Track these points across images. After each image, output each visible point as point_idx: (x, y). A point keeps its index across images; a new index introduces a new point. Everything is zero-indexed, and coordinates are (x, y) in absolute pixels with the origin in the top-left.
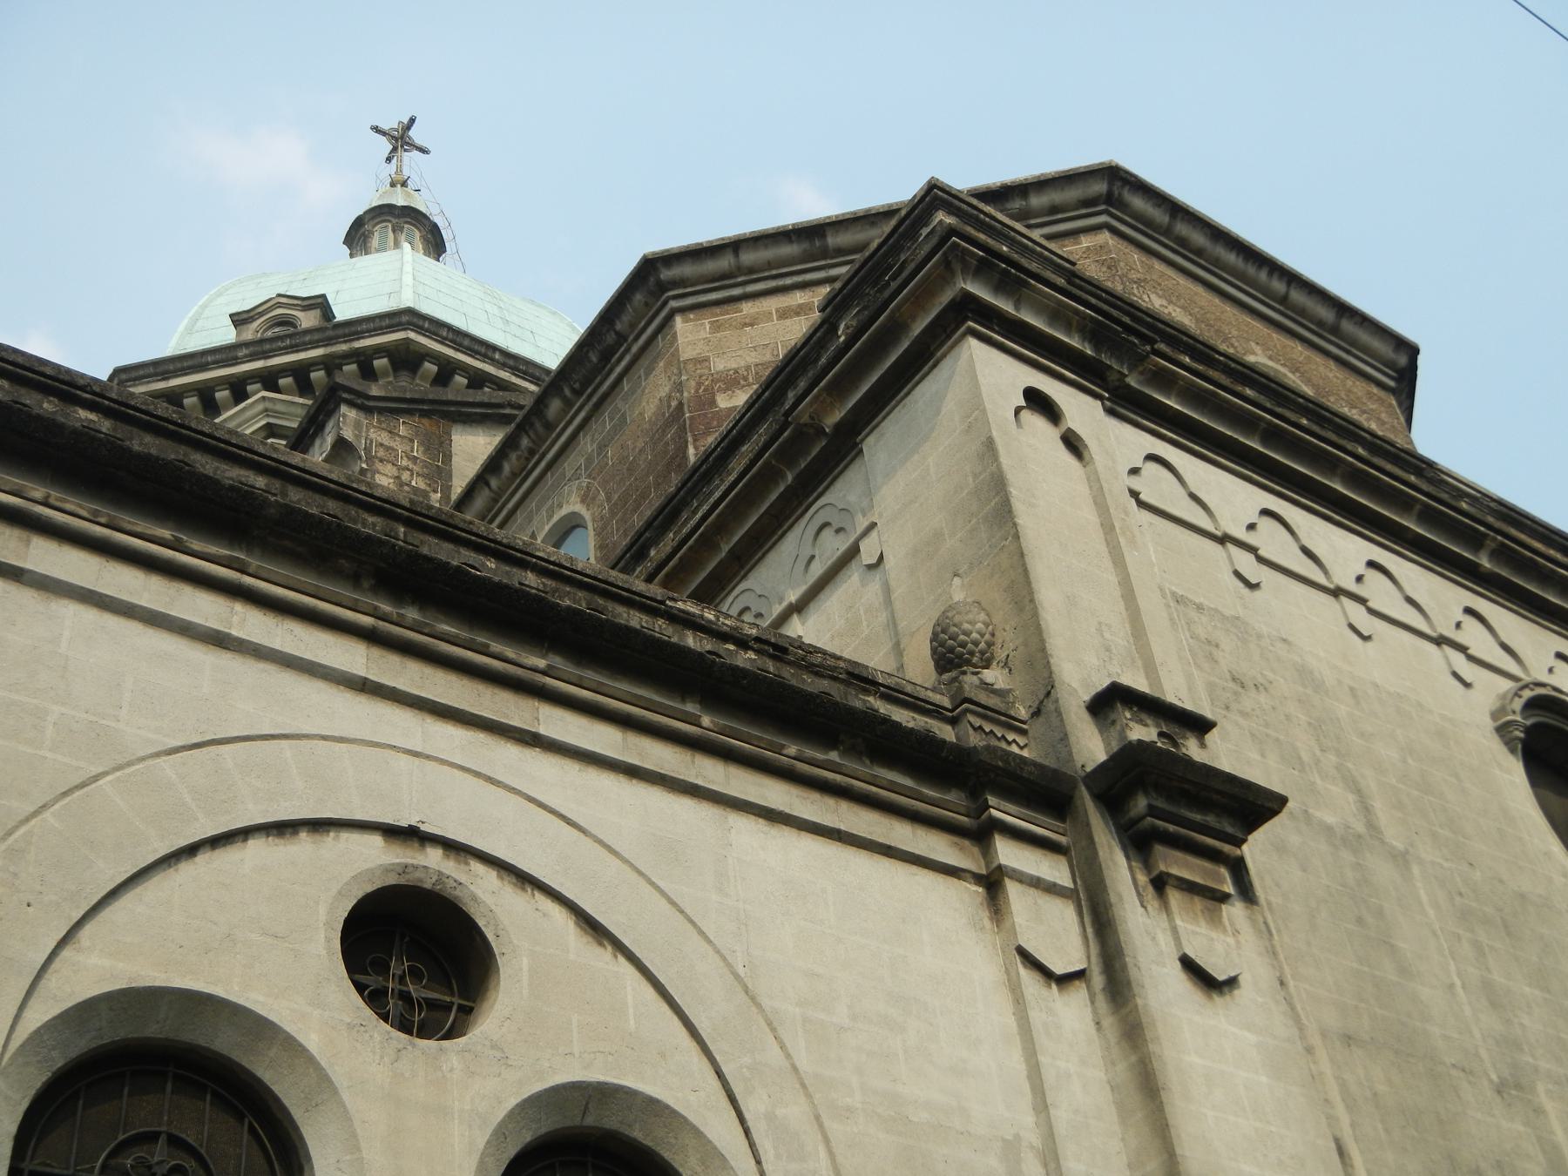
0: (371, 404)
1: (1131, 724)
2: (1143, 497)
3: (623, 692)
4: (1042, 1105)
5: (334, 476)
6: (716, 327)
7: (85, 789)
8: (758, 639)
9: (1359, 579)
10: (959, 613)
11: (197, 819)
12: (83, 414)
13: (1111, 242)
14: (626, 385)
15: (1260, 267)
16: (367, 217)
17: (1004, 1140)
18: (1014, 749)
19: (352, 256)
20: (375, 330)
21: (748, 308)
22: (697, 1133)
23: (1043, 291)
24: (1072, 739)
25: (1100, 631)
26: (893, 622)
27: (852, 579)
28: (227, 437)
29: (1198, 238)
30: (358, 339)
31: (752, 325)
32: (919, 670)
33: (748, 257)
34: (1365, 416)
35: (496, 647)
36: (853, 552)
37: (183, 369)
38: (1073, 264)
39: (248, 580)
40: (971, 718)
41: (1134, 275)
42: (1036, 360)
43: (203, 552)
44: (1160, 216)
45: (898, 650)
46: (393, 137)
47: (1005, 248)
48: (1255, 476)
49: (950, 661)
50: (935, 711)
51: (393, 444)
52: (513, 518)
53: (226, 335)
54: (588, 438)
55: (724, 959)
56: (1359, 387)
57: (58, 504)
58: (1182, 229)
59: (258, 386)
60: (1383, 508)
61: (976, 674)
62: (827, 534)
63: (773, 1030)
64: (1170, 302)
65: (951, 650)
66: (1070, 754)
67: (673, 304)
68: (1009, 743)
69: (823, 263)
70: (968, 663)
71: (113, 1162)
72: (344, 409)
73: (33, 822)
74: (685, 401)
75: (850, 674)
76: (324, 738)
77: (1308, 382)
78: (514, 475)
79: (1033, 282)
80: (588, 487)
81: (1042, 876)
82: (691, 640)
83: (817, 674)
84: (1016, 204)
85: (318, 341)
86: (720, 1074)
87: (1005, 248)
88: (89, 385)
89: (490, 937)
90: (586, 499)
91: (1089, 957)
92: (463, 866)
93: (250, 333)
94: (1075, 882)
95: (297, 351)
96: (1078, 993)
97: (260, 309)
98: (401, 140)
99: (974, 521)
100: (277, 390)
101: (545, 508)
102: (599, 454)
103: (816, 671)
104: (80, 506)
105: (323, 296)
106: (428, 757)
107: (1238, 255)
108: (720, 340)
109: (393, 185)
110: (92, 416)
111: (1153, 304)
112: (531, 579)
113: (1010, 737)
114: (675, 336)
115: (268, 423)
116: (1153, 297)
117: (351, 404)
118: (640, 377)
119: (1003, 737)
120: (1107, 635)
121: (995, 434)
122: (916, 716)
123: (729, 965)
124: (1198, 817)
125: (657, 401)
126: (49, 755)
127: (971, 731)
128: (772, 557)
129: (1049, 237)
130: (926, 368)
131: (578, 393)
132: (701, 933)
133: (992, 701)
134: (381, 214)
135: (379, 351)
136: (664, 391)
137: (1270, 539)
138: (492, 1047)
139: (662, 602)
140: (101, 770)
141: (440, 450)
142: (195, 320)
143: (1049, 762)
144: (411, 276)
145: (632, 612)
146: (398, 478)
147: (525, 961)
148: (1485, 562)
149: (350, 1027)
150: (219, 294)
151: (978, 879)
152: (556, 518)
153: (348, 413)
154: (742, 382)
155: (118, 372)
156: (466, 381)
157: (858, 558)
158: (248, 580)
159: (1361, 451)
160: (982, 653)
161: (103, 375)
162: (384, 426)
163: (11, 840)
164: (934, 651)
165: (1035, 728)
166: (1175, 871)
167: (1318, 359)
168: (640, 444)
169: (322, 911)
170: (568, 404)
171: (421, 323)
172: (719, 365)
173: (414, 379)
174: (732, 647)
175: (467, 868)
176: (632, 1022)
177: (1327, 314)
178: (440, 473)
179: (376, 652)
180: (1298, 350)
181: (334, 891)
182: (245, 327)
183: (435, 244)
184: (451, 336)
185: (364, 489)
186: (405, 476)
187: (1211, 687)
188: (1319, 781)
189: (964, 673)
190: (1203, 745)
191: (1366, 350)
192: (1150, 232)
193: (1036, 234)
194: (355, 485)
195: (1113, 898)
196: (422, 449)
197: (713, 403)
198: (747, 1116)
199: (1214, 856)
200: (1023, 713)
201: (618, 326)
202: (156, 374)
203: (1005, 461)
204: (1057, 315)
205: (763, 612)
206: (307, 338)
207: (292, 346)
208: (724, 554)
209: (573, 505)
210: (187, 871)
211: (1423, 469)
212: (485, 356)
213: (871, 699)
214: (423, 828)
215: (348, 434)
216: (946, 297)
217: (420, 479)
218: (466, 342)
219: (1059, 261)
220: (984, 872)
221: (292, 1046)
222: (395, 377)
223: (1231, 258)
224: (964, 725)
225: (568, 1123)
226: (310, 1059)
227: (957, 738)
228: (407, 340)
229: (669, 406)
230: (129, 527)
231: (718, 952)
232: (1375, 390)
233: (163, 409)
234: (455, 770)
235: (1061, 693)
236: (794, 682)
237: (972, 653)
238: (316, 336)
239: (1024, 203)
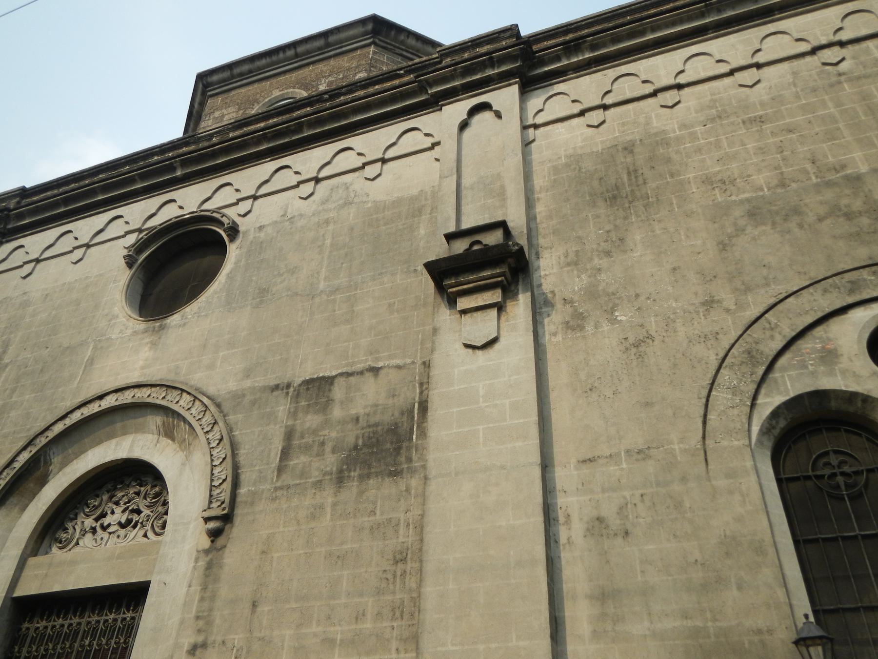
29: (245, 68)
44: (226, 74)
58: (237, 71)
107: (266, 58)
148: (179, 173)
191: (347, 39)
211: (187, 141)
223: (264, 62)
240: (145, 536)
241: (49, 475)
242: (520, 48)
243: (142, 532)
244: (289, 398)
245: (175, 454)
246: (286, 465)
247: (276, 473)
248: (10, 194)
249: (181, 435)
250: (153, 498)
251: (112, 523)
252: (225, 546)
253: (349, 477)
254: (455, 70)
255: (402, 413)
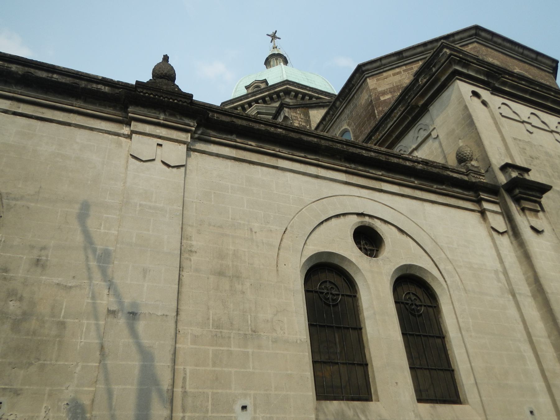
0: (291, 107)
1: (512, 172)
2: (503, 114)
3: (398, 178)
4: (501, 261)
5: (329, 136)
6: (378, 80)
7: (301, 212)
8: (422, 161)
9: (557, 127)
10: (463, 149)
11: (322, 216)
12: (279, 130)
13: (477, 45)
14: (356, 97)
15: (516, 46)
16: (269, 57)
17: (495, 270)
18: (482, 180)
19: (267, 68)
20: (279, 86)
21: (385, 74)
22: (430, 273)
23: (474, 66)
24: (497, 177)
25: (498, 149)
26: (443, 151)
27: (430, 142)
28: (307, 131)
29: (499, 41)
30: (275, 89)
31: (386, 79)
32: (452, 162)
33: (384, 62)
34: (545, 81)
35: (371, 171)
36: (430, 135)
37: (237, 101)
38: (478, 56)
39: (320, 163)
40: (472, 174)
41: (484, 54)
42: (473, 83)
43: (311, 158)
44: (489, 37)
45: (445, 157)
46: (272, 36)
47: (461, 55)
49: (462, 160)
50: (462, 173)
51: (297, 116)
52: (330, 131)
53: (244, 92)
54: (347, 110)
55: (429, 235)
56: (543, 74)
57: (281, 151)
58: (495, 39)
59: (254, 103)
61: (470, 163)
62: (421, 131)
63: (442, 250)
64: (494, 59)
65: (462, 158)
66: (497, 180)
67: (366, 76)
68: (481, 179)
69: (402, 61)
70: (467, 160)
71: (320, 287)
72: (285, 109)
73: (293, 220)
74: (372, 99)
75: (443, 167)
76: (341, 195)
77: (530, 74)
78: (329, 121)
79: (471, 64)
80: (349, 122)
81: (494, 210)
82: (408, 163)
83: (436, 168)
84: (451, 39)
85: (266, 90)
86: (433, 260)
87: (461, 55)
88: (279, 123)
89: (381, 235)
90: (349, 125)
91: (507, 227)
92: (373, 220)
93: (250, 90)
94: (502, 210)
95: (262, 94)
96: (506, 236)
97: (251, 84)
98: (274, 37)
99: (464, 126)
100: (259, 103)
101: (338, 128)
102: (351, 114)
103: (435, 167)
104: (286, 151)
105: (266, 79)
106: (362, 197)
108: (379, 83)
109: (274, 48)
110: (281, 130)
111: (489, 60)
112: (373, 154)
113: (481, 177)
114: (367, 83)
115: (258, 112)
116: (489, 58)
117: (286, 107)
118: (359, 94)
119: (480, 178)
120: (500, 150)
121: (467, 104)
122: (458, 175)
123: (430, 237)
124: (531, 193)
125: (365, 100)
126: (292, 205)
127: (472, 177)
128: (406, 137)
129: (461, 46)
130: (445, 89)
131: (343, 100)
132: (423, 230)
133: (476, 169)
134: (272, 56)
135: (281, 91)
136: (366, 97)
137: (535, 121)
138: (387, 259)
139: (400, 156)
140: (302, 207)
141: (307, 115)
142: (236, 89)
143: (492, 183)
144: (285, 72)
145: (394, 159)
146: (299, 123)
147: (389, 240)
149: (360, 256)
150: (241, 82)
151: (479, 212)
152: (341, 130)
153: (286, 110)
154: (386, 93)
155: (222, 103)
156: (308, 98)
157: (431, 136)
158: (320, 163)
159: (552, 93)
160: (470, 158)
161: (219, 105)
162: (294, 111)
163: (290, 224)
164: (457, 158)
165: (487, 175)
166: (527, 206)
167: (532, 68)
168: (362, 111)
169: (349, 232)
170: (341, 102)
171: (290, 83)
172: (380, 89)
173: (289, 97)
174: (416, 164)
175: (373, 220)
176: (413, 251)
177: (533, 56)
178: (308, 121)
179: (347, 175)
180: (527, 66)
181: (350, 228)
182: (248, 89)
183: (286, 62)
184: (297, 85)
185: (336, 138)
186: (301, 123)
187: (526, 160)
188: (554, 180)
189: (467, 163)
190: (529, 175)
191: (544, 63)
192: (487, 41)
193: (457, 46)
194: (334, 138)
195: (513, 214)
196: (303, 116)
197: (379, 99)
198: (440, 269)
199: (535, 202)
200: (483, 171)
201: (353, 83)
202: (231, 103)
203: (471, 110)
204: (478, 71)
205: (406, 150)
206: (264, 90)
207: (261, 93)
208: (394, 138)
209: (345, 127)
210: (322, 227)
212: (305, 89)
213: (448, 172)
214: (364, 213)
215: (287, 115)
216: (450, 71)
217: (304, 123)
218: (301, 86)
219: (474, 56)
220: (480, 210)
221: (350, 262)
222: (285, 97)
223: (508, 45)
224: (470, 176)
225: (404, 273)
226: (354, 264)
227: (468, 179)
228: (287, 88)
229: (368, 101)
230: (295, 154)
231: (427, 234)
232: (547, 74)
233: (236, 112)
234: (367, 199)
235: (493, 166)
236: (431, 170)
237: (467, 158)
238: (266, 89)
239: (453, 38)
248: (471, 55)
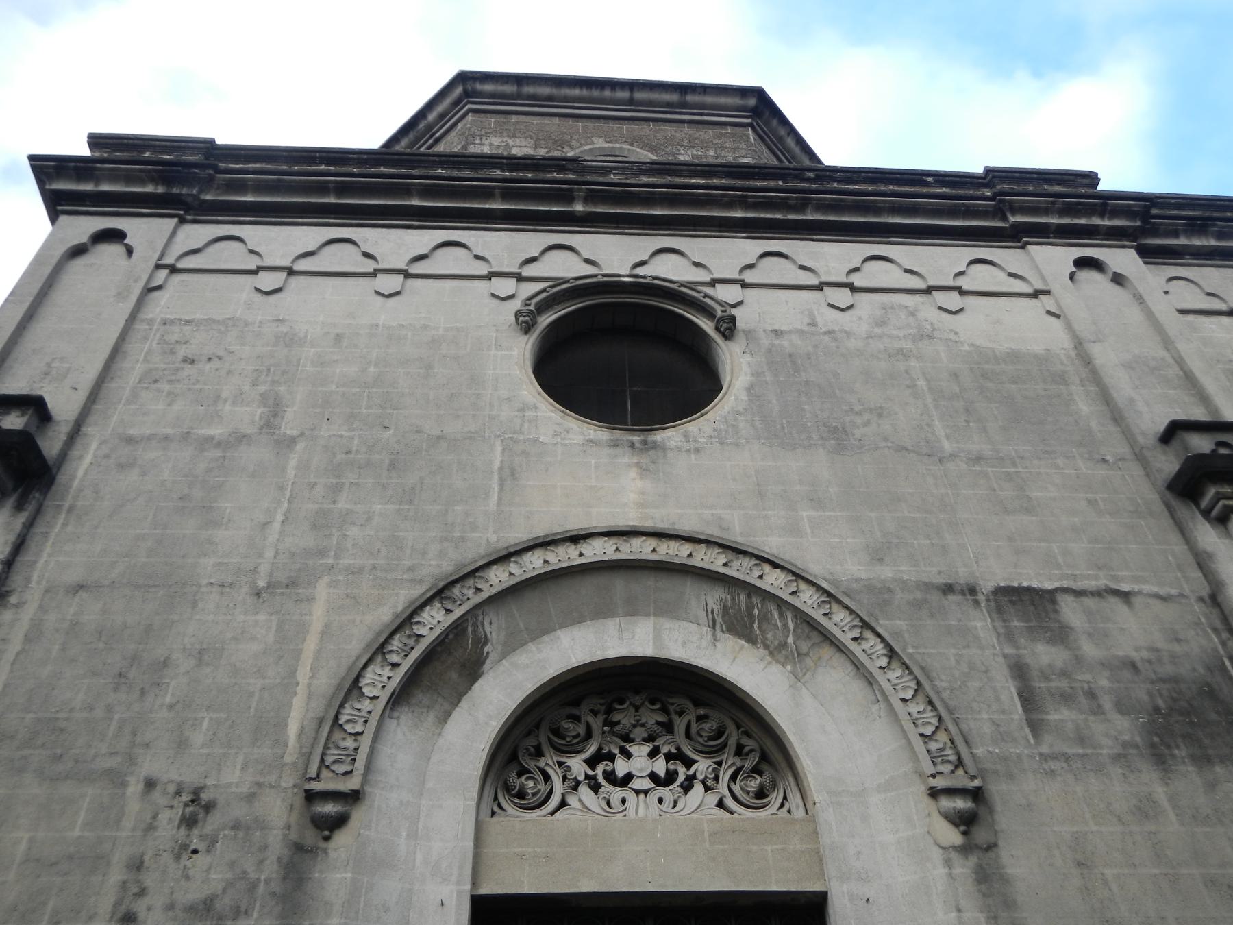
29: (545, 90)
48: (332, 221)
58: (529, 89)
60: (465, 203)
79: (99, 165)
84: (422, 125)
148: (579, 208)
177: (673, 97)
204: (129, 179)
211: (564, 165)
223: (576, 92)
240: (720, 804)
241: (483, 663)
242: (1145, 205)
243: (712, 799)
244: (984, 610)
245: (766, 667)
246: (1043, 720)
247: (1027, 730)
249: (775, 636)
250: (710, 739)
251: (635, 773)
252: (995, 845)
253: (1173, 756)
254: (1053, 203)
255: (1209, 669)
